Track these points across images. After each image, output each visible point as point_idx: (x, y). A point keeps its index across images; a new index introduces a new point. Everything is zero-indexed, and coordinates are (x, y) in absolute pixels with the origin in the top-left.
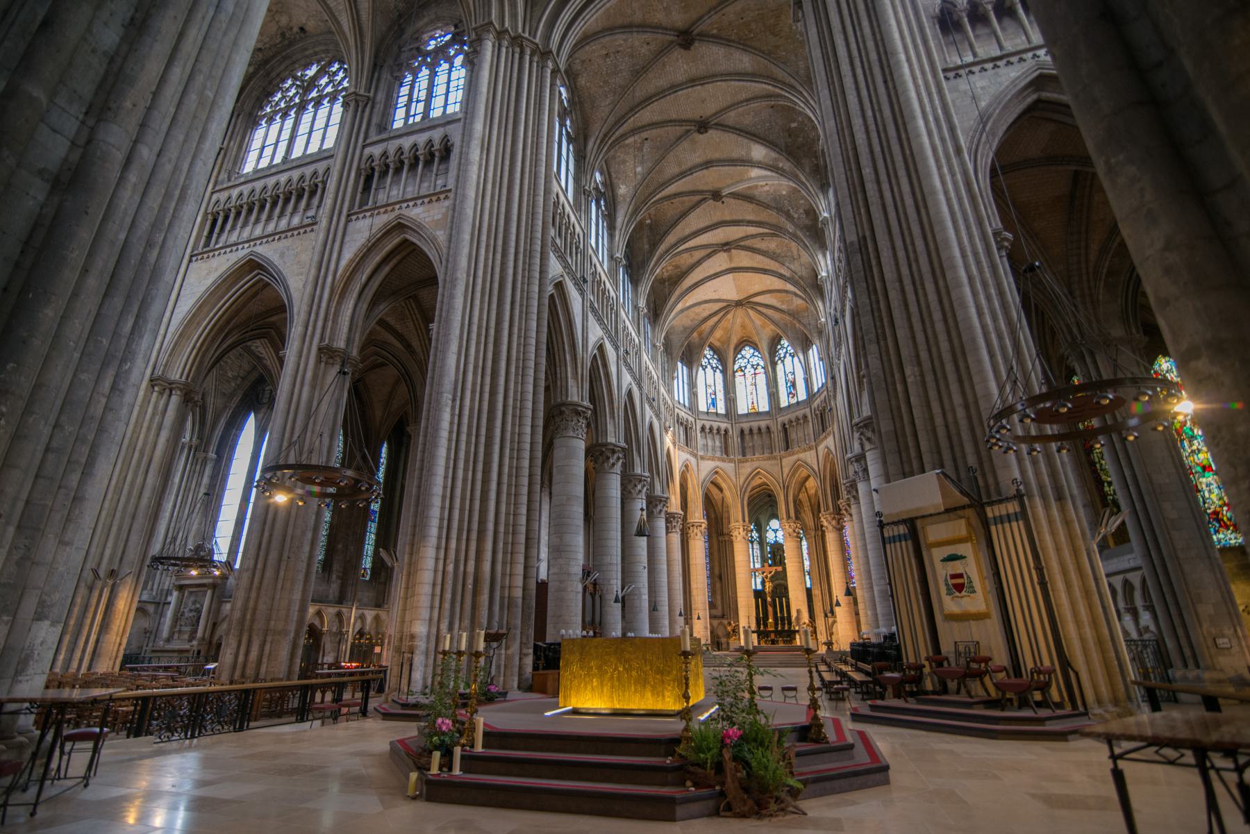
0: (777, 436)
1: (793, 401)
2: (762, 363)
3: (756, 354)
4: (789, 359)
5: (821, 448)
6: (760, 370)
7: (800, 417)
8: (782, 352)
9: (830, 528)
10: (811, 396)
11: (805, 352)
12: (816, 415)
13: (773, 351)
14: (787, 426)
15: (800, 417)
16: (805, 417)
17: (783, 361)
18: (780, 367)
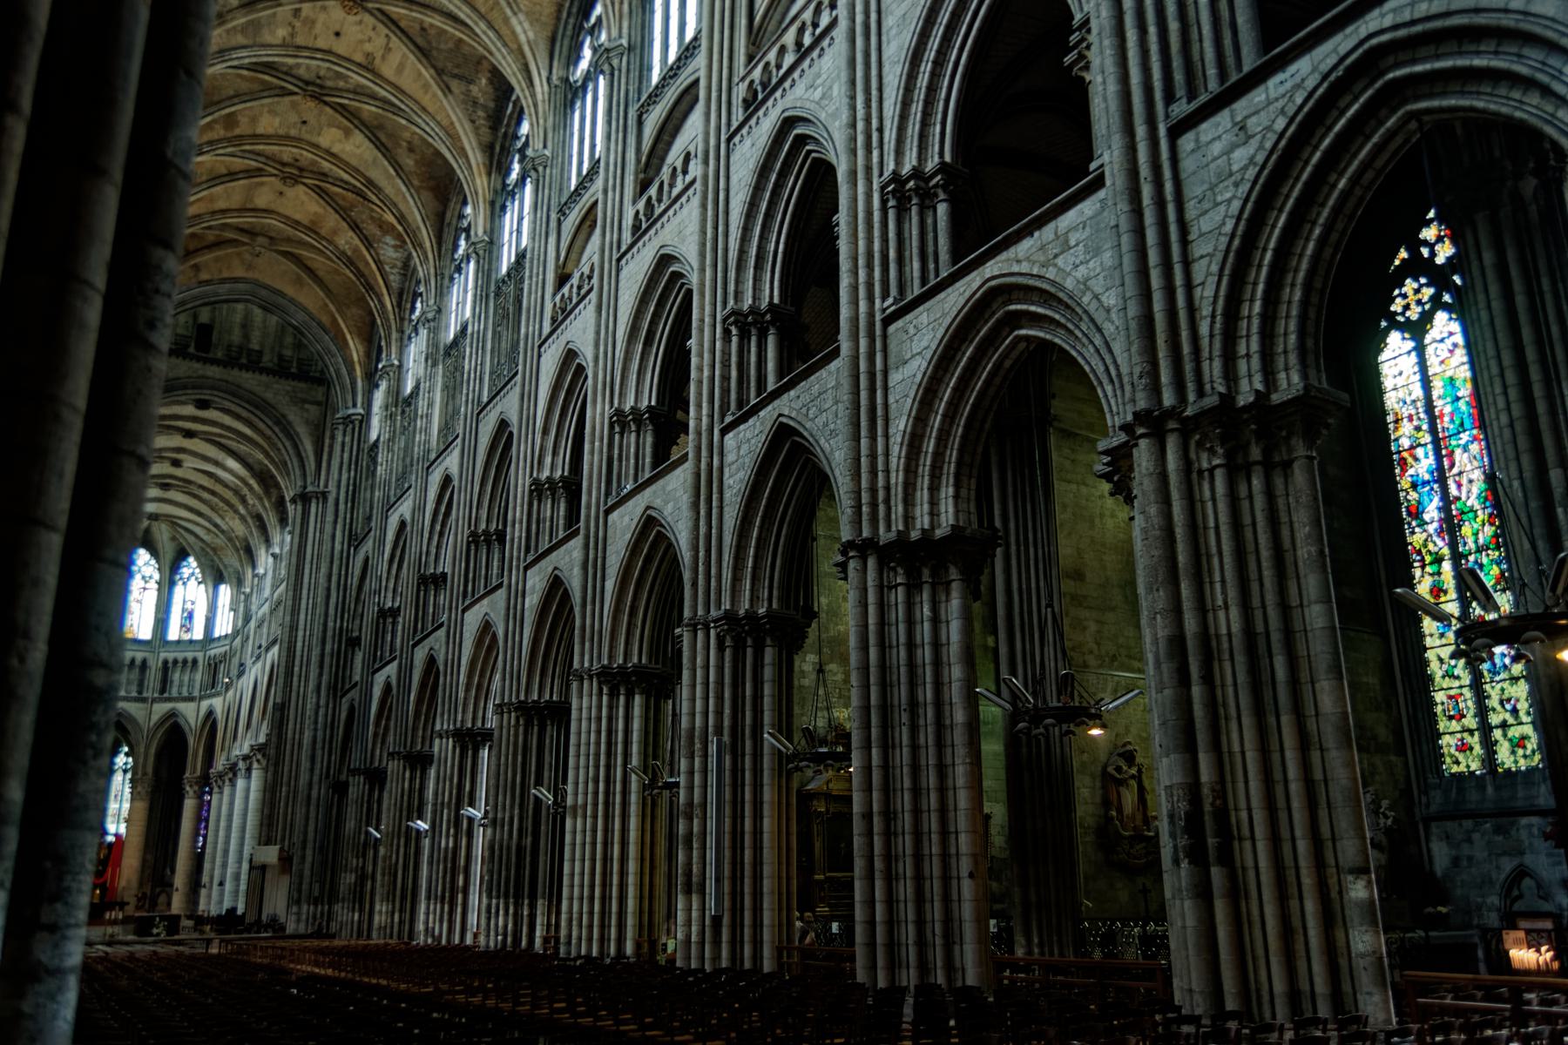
0: (153, 677)
1: (186, 637)
2: (157, 576)
3: (153, 562)
4: (193, 582)
5: (205, 704)
6: (153, 585)
7: (190, 659)
8: (185, 572)
9: (191, 793)
10: (209, 638)
11: (216, 587)
12: (209, 665)
13: (175, 568)
14: (170, 665)
15: (190, 659)
16: (195, 661)
17: (184, 583)
18: (179, 590)
